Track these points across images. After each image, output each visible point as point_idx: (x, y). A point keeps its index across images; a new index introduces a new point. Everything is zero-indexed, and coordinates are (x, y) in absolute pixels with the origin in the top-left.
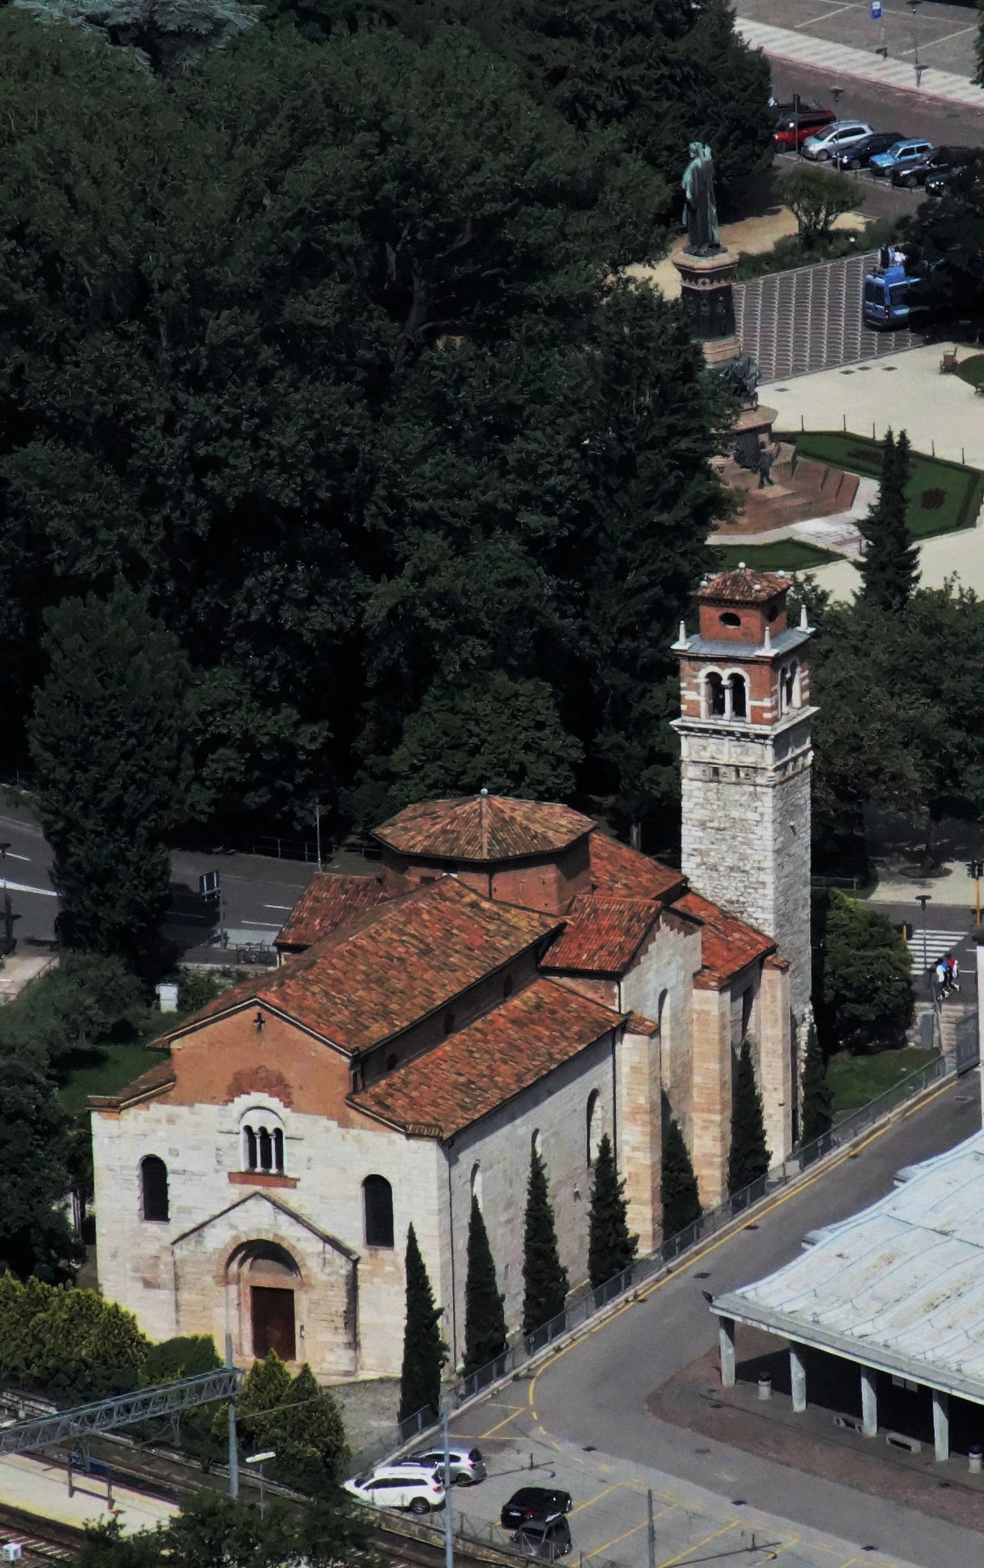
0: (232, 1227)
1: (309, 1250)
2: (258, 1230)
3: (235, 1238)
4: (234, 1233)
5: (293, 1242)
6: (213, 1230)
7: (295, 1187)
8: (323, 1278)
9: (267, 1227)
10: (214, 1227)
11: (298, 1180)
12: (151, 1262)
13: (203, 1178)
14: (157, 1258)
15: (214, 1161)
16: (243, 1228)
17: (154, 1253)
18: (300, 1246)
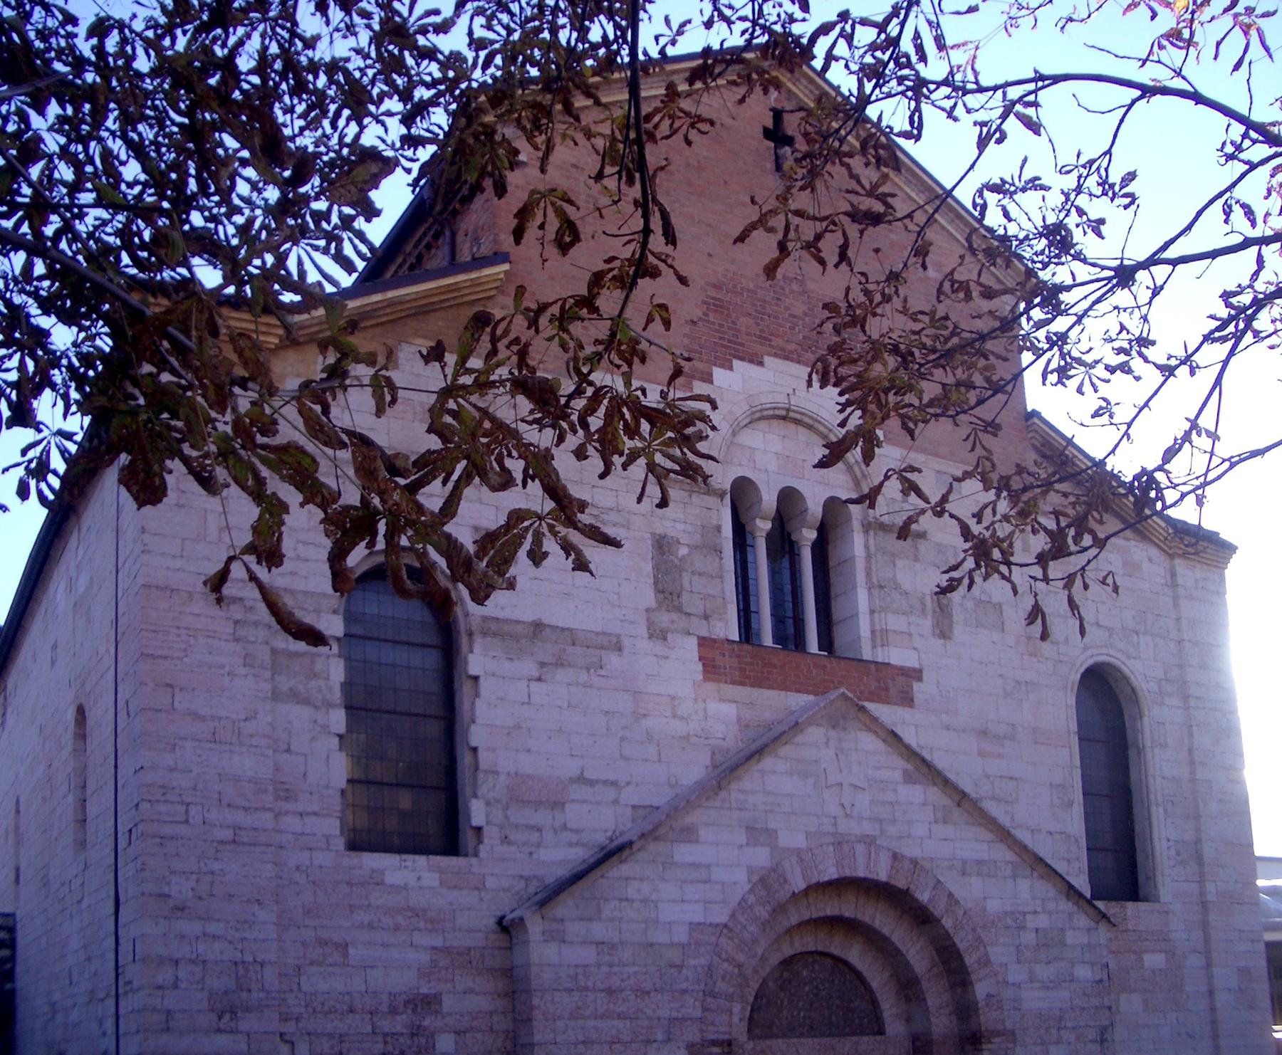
0: (757, 833)
1: (994, 906)
2: (840, 842)
3: (765, 881)
4: (761, 857)
5: (953, 885)
6: (684, 853)
7: (907, 700)
8: (1034, 999)
9: (868, 828)
10: (689, 834)
11: (917, 674)
12: (399, 1024)
13: (613, 660)
14: (429, 1003)
15: (648, 597)
16: (792, 838)
17: (403, 981)
18: (970, 890)
